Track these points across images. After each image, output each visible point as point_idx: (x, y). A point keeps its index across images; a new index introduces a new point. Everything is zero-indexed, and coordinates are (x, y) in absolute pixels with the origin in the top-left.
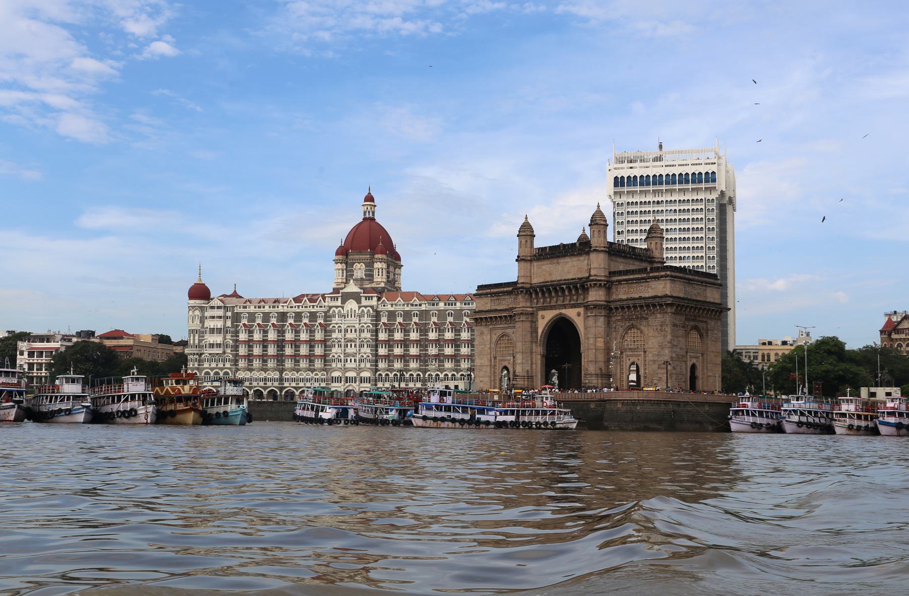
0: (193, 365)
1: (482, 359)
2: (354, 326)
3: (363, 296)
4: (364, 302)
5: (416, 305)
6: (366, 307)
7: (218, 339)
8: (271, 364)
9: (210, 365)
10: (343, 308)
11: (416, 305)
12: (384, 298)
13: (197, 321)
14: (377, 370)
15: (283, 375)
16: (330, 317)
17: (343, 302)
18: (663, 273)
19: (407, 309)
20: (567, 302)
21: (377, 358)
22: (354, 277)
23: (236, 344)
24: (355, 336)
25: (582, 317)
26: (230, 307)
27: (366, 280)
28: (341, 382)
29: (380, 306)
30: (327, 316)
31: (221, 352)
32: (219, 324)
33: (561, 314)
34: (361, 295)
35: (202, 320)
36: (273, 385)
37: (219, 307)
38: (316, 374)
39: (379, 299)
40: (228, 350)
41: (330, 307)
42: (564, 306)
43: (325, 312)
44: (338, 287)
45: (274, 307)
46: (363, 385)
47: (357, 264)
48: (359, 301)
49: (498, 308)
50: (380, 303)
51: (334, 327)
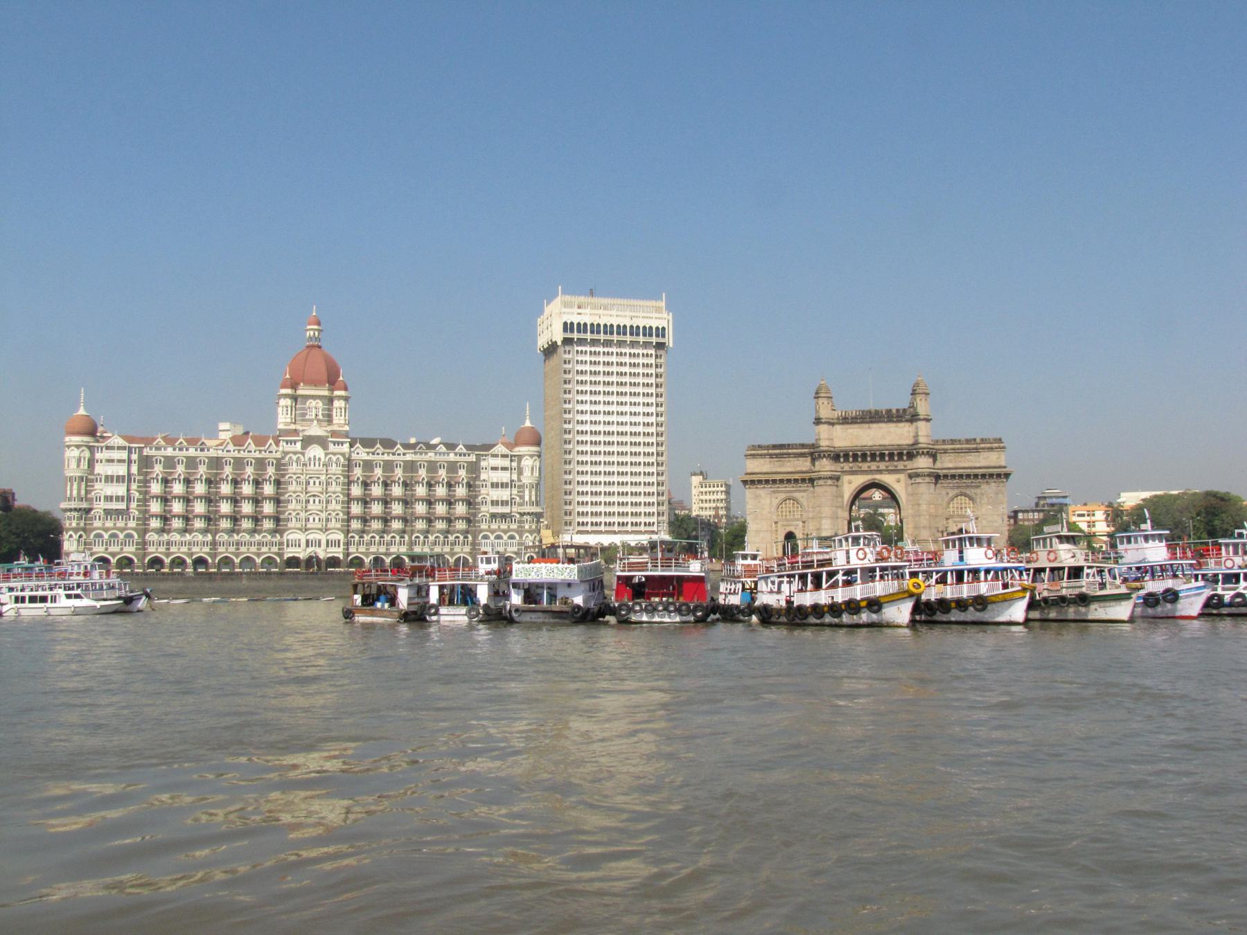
0: (70, 524)
1: (758, 524)
2: (318, 478)
3: (331, 442)
4: (332, 448)
5: (399, 454)
6: (334, 454)
7: (121, 490)
8: (199, 524)
9: (104, 524)
10: (303, 454)
11: (399, 454)
12: (358, 445)
13: (84, 465)
14: (348, 532)
15: (217, 538)
16: (284, 465)
17: (304, 447)
18: (996, 445)
19: (386, 457)
20: (884, 468)
21: (349, 518)
22: (307, 417)
23: (145, 498)
24: (320, 490)
25: (902, 484)
26: (135, 448)
27: (324, 421)
28: (299, 546)
29: (353, 454)
30: (280, 465)
31: (125, 507)
32: (122, 470)
33: (874, 479)
34: (330, 439)
35: (91, 463)
36: (202, 551)
37: (119, 448)
38: (264, 537)
39: (351, 446)
40: (134, 505)
41: (286, 453)
42: (880, 472)
43: (278, 460)
44: (287, 427)
45: (202, 450)
46: (330, 549)
47: (312, 401)
48: (324, 445)
49: (779, 470)
50: (352, 450)
51: (291, 477)
